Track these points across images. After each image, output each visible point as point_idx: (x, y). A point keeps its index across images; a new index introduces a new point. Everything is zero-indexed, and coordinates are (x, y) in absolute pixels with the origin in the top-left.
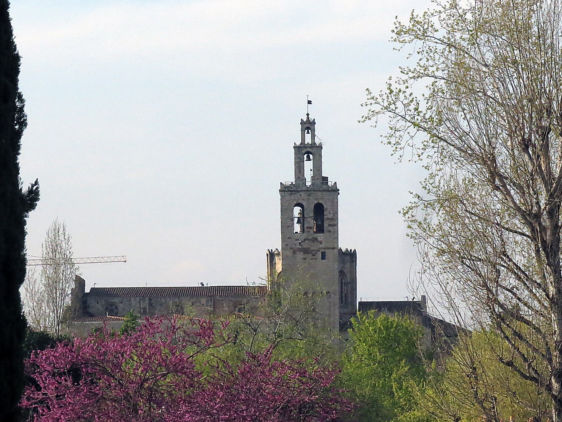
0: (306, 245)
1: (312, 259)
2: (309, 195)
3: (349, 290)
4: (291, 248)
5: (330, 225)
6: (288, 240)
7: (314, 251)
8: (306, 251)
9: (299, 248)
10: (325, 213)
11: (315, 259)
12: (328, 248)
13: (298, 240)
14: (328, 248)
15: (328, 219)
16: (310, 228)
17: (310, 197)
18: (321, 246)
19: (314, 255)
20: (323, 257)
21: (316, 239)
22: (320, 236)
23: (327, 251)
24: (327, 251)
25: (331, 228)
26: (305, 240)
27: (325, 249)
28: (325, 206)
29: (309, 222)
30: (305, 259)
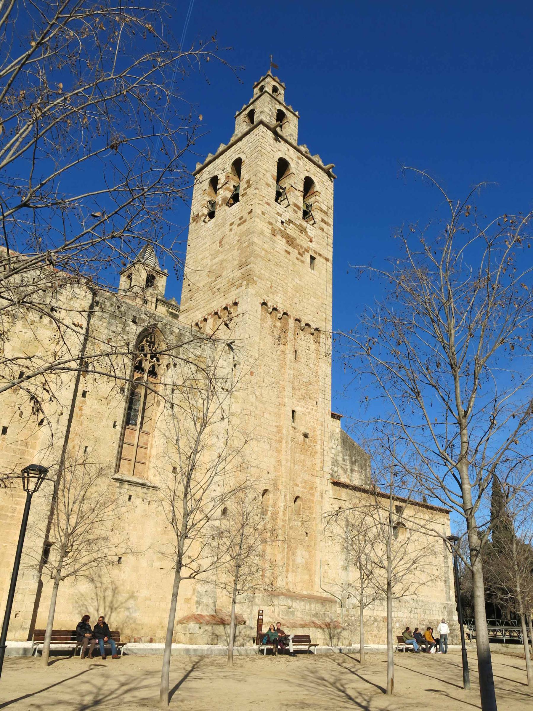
1: (297, 259)
4: (271, 224)
5: (323, 221)
6: (267, 206)
8: (290, 241)
9: (280, 230)
12: (320, 255)
13: (281, 215)
14: (320, 255)
15: (321, 210)
17: (301, 163)
19: (302, 256)
27: (316, 253)
30: (289, 253)
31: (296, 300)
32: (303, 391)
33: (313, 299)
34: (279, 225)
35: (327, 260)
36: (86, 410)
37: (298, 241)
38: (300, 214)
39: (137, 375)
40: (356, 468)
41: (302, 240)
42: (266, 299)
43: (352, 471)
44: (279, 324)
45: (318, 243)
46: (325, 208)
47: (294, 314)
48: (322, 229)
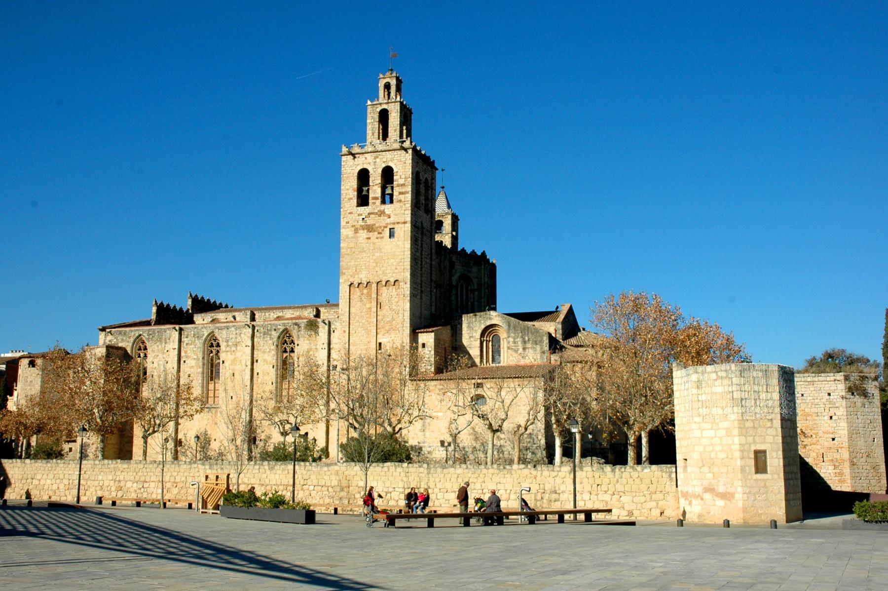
0: (370, 222)
2: (375, 158)
3: (476, 298)
5: (400, 193)
7: (380, 227)
8: (370, 229)
10: (395, 178)
11: (382, 238)
12: (398, 223)
14: (398, 223)
15: (398, 186)
16: (376, 198)
17: (378, 160)
18: (388, 221)
20: (391, 235)
21: (382, 213)
22: (388, 208)
23: (396, 226)
24: (396, 226)
25: (402, 197)
27: (394, 224)
28: (395, 170)
29: (375, 192)
30: (369, 238)
31: (377, 269)
32: (387, 328)
33: (392, 260)
34: (361, 223)
35: (405, 223)
36: (260, 380)
37: (377, 225)
38: (379, 202)
39: (285, 355)
40: (529, 345)
41: (382, 221)
42: (352, 280)
43: (524, 349)
44: (365, 291)
45: (396, 215)
46: (401, 181)
47: (374, 280)
48: (400, 201)
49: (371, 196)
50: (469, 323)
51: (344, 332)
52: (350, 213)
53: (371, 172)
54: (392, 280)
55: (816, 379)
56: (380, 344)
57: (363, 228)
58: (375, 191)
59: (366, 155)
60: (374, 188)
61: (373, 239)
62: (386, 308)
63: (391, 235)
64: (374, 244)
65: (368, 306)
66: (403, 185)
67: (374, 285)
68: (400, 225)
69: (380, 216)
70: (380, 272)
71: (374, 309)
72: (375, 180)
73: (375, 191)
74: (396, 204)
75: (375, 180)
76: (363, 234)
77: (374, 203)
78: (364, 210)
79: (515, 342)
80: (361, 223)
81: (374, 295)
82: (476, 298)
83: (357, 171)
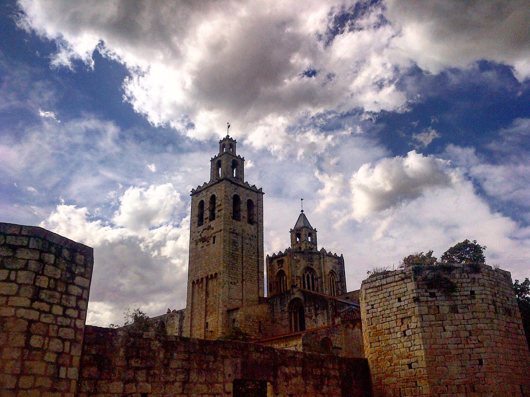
5: (219, 211)
7: (208, 237)
8: (203, 240)
12: (217, 232)
14: (217, 232)
17: (208, 193)
20: (214, 243)
21: (209, 228)
22: (213, 224)
23: (217, 234)
25: (219, 214)
26: (203, 230)
27: (215, 233)
35: (221, 231)
42: (193, 278)
43: (316, 315)
49: (205, 217)
50: (281, 301)
51: (189, 317)
52: (194, 232)
53: (205, 202)
54: (213, 273)
55: (384, 282)
56: (207, 323)
57: (200, 240)
58: (207, 214)
59: (203, 192)
60: (206, 212)
61: (205, 247)
62: (211, 295)
63: (214, 243)
64: (205, 250)
65: (201, 296)
66: (220, 205)
67: (205, 280)
68: (219, 233)
69: (208, 230)
70: (207, 270)
71: (204, 298)
72: (207, 206)
73: (207, 214)
74: (217, 219)
75: (207, 206)
76: (200, 244)
77: (206, 222)
78: (201, 228)
79: (309, 311)
80: (199, 237)
81: (204, 287)
82: (319, 284)
83: (198, 203)
